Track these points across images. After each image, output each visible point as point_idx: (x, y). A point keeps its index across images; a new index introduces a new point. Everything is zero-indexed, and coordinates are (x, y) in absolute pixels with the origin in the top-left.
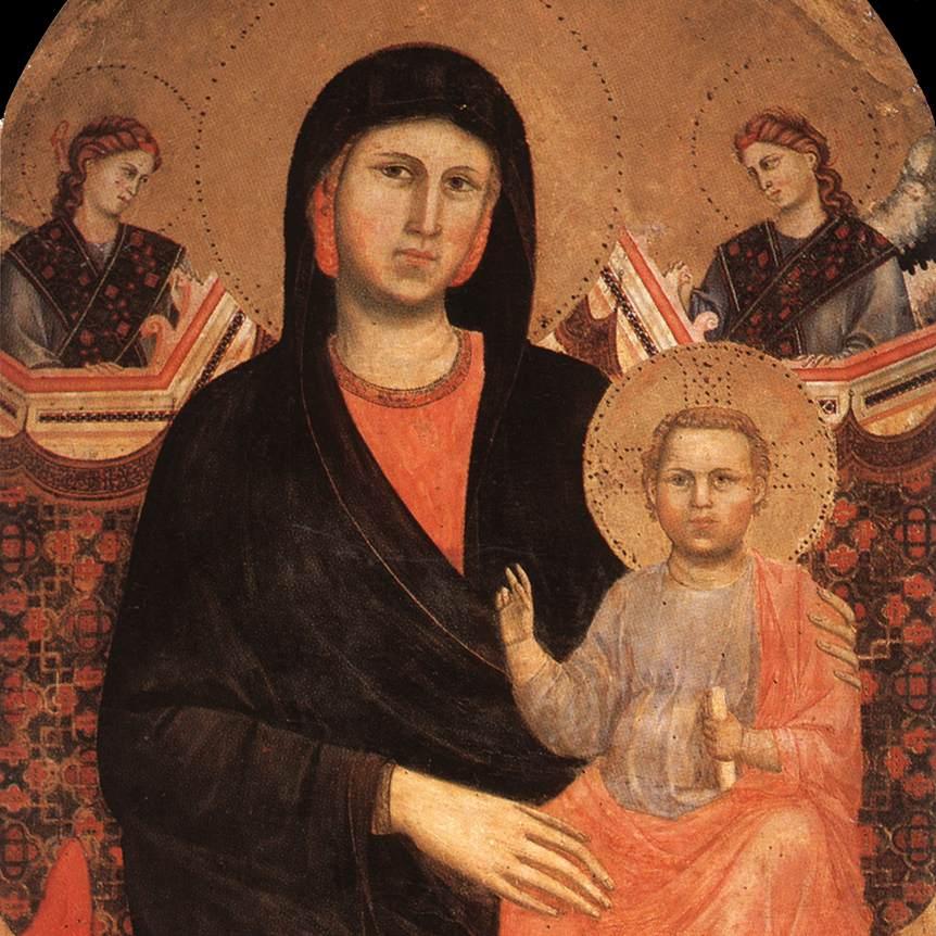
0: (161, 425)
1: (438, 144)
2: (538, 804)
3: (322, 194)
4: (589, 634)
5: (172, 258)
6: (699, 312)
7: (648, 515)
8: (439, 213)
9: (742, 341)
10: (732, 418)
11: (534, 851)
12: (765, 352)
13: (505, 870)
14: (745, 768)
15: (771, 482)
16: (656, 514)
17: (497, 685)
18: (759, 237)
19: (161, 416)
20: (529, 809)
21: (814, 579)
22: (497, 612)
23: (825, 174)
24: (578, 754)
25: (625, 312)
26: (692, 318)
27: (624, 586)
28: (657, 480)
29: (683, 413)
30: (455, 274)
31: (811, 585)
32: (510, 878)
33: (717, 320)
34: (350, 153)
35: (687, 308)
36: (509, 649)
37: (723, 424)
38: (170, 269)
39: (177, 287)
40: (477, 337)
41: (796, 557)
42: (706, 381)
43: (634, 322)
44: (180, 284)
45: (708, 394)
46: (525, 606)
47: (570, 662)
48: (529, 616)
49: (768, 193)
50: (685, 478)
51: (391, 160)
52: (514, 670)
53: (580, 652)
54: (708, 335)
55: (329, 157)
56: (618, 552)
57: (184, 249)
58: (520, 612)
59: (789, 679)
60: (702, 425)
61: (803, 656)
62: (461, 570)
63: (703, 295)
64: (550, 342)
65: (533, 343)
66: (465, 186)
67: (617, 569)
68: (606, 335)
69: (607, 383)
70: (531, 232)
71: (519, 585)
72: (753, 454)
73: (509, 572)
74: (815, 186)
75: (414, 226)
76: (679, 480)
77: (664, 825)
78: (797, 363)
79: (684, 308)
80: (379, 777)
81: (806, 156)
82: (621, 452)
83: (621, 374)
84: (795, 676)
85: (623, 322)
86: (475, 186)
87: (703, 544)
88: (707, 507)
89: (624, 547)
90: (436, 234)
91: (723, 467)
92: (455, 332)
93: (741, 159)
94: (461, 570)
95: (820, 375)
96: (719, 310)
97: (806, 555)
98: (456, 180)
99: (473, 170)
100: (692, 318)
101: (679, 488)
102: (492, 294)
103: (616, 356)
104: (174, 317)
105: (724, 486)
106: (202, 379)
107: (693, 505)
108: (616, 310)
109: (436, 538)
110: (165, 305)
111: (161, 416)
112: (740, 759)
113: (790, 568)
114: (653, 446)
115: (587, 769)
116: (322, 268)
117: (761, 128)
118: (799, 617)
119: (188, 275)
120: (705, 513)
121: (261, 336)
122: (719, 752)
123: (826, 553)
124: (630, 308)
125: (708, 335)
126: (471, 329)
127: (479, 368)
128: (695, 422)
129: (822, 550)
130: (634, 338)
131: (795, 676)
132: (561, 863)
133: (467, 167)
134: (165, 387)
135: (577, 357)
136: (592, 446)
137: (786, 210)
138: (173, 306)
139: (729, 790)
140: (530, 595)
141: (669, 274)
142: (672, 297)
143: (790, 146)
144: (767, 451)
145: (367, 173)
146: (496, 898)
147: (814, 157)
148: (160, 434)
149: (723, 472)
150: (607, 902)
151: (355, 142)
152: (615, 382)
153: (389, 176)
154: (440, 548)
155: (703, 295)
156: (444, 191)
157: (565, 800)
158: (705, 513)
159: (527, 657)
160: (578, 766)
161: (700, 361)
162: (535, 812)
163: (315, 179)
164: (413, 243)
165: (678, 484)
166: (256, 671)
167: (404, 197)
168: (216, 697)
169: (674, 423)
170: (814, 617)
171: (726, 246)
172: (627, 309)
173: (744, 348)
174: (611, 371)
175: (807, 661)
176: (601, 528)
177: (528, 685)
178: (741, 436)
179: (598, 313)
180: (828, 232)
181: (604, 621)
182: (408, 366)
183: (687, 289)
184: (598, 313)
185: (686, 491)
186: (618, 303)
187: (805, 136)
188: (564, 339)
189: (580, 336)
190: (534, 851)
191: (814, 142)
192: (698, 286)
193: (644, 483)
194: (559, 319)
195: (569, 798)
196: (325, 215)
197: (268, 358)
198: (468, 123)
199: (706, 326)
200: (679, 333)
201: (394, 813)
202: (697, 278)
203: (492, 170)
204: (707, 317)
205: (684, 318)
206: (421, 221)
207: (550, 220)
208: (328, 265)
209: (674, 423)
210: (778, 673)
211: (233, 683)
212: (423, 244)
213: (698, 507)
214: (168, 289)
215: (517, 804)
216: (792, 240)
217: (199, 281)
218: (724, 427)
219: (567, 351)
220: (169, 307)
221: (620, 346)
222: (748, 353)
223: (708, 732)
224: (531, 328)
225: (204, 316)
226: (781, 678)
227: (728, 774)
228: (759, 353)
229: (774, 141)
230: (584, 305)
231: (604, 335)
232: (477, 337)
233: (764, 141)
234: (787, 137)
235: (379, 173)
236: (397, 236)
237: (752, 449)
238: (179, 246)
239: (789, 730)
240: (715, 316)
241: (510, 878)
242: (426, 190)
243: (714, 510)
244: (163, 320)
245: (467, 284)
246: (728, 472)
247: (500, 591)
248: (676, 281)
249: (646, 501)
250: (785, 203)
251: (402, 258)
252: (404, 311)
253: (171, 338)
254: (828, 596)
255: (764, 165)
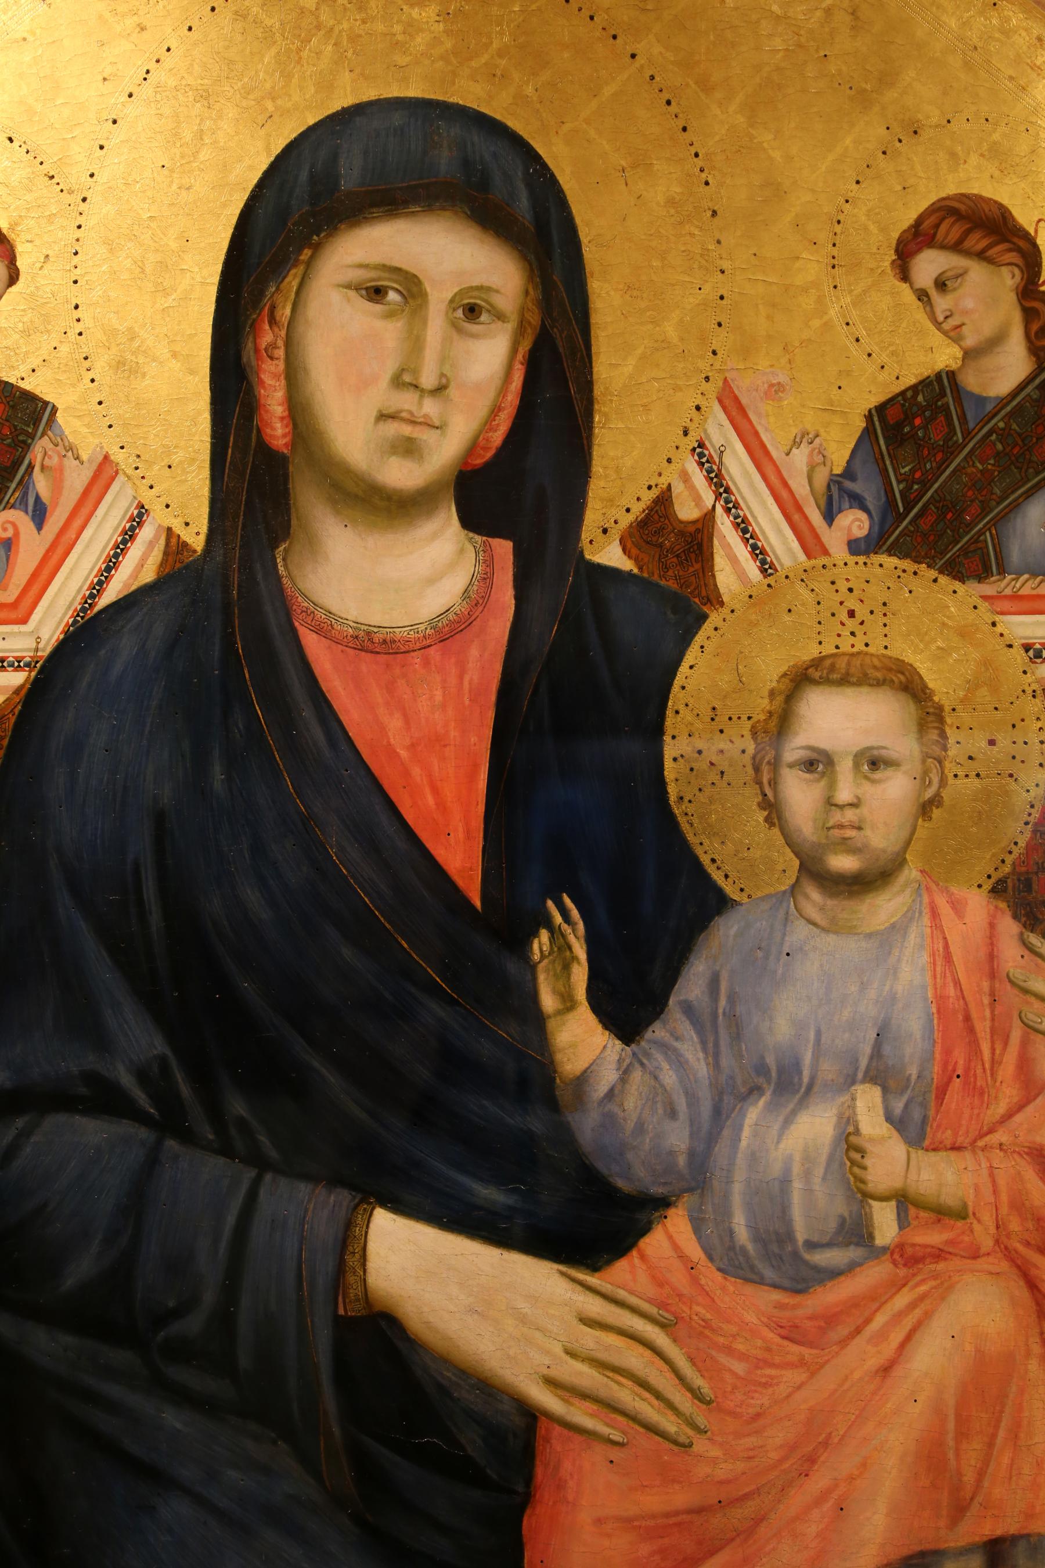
0: (17, 679)
1: (448, 253)
2: (595, 1268)
3: (267, 327)
4: (671, 1002)
5: (36, 422)
6: (840, 511)
7: (761, 819)
8: (443, 359)
9: (904, 555)
10: (890, 670)
11: (590, 1339)
12: (941, 572)
13: (546, 1371)
14: (912, 1211)
15: (950, 768)
16: (774, 815)
17: (535, 1078)
18: (938, 393)
19: (18, 665)
20: (581, 1276)
21: (1015, 917)
22: (533, 968)
23: (1035, 299)
24: (657, 1190)
25: (728, 511)
26: (829, 517)
27: (726, 930)
28: (775, 765)
29: (817, 662)
30: (473, 448)
31: (1009, 927)
32: (551, 1383)
33: (867, 525)
34: (309, 264)
35: (823, 502)
36: (551, 1024)
37: (878, 681)
38: (32, 436)
39: (43, 468)
40: (504, 548)
41: (988, 885)
42: (851, 614)
43: (743, 526)
44: (47, 462)
45: (853, 634)
46: (575, 958)
47: (643, 1043)
48: (580, 975)
49: (946, 326)
50: (817, 763)
51: (373, 274)
52: (559, 1057)
53: (657, 1032)
54: (855, 547)
55: (278, 266)
56: (717, 877)
57: (54, 410)
58: (566, 967)
59: (979, 1071)
60: (844, 681)
61: (1000, 1034)
62: (478, 903)
63: (848, 484)
64: (611, 555)
65: (588, 557)
66: (484, 317)
67: (721, 903)
68: (700, 545)
69: (704, 617)
70: (587, 385)
71: (565, 926)
72: (922, 727)
73: (550, 903)
74: (1017, 317)
75: (407, 378)
76: (810, 765)
77: (787, 1301)
78: (988, 589)
79: (819, 508)
80: (349, 1225)
81: (1005, 270)
82: (722, 720)
83: (722, 604)
84: (987, 1066)
85: (724, 524)
86: (500, 316)
87: (843, 863)
88: (851, 805)
89: (727, 868)
90: (439, 390)
91: (875, 744)
92: (470, 540)
93: (904, 274)
94: (478, 903)
95: (1025, 605)
96: (871, 507)
97: (1002, 881)
98: (472, 309)
99: (497, 291)
100: (829, 517)
101: (807, 776)
102: (522, 482)
103: (714, 576)
104: (39, 515)
105: (878, 775)
106: (84, 610)
107: (830, 803)
108: (714, 507)
109: (440, 853)
110: (25, 494)
111: (18, 665)
112: (905, 1201)
113: (978, 904)
114: (770, 712)
115: (671, 1212)
116: (267, 439)
117: (937, 226)
118: (993, 975)
119: (60, 448)
120: (850, 815)
121: (174, 546)
122: (871, 1187)
123: (1035, 878)
124: (736, 506)
125: (855, 547)
126: (493, 537)
127: (506, 597)
128: (835, 676)
129: (1027, 873)
130: (742, 552)
131: (987, 1066)
132: (635, 1359)
133: (489, 289)
134: (24, 621)
135: (656, 578)
136: (677, 712)
137: (969, 355)
138: (38, 498)
139: (884, 1249)
140: (583, 941)
141: (794, 450)
142: (800, 487)
143: (981, 256)
144: (941, 720)
145: (336, 297)
146: (531, 1415)
147: (1017, 271)
148: (17, 691)
149: (875, 752)
150: (701, 1421)
151: (317, 248)
152: (714, 618)
153: (370, 300)
154: (445, 867)
155: (848, 484)
156: (455, 325)
157: (637, 1261)
158: (850, 815)
159: (580, 1040)
160: (656, 1209)
161: (843, 586)
162: (592, 1280)
163: (256, 301)
164: (406, 401)
165: (809, 771)
166: (163, 1060)
167: (390, 333)
168: (103, 1099)
169: (802, 679)
170: (1017, 974)
171: (881, 408)
172: (731, 507)
173: (906, 564)
174: (708, 601)
175: (1006, 1043)
176: (690, 838)
177: (582, 1080)
178: (902, 696)
179: (686, 511)
180: (1037, 387)
181: (692, 984)
182: (394, 584)
183: (821, 478)
184: (686, 511)
185: (818, 781)
186: (718, 496)
187: (1004, 240)
188: (634, 551)
189: (661, 546)
190: (590, 1339)
191: (1019, 250)
192: (838, 470)
193: (757, 769)
194: (626, 521)
195: (643, 1257)
196: (272, 358)
197: (179, 571)
198: (489, 217)
199: (849, 529)
200: (812, 545)
201: (371, 1280)
202: (839, 458)
203: (527, 293)
204: (851, 518)
205: (816, 517)
206: (416, 372)
207: (613, 367)
208: (277, 432)
209: (802, 679)
210: (961, 1062)
211: (127, 1080)
212: (420, 404)
213: (836, 805)
214: (31, 467)
215: (562, 1268)
216: (981, 400)
217: (77, 458)
218: (879, 684)
219: (640, 568)
220: (31, 501)
221: (720, 561)
222: (915, 573)
223: (857, 1156)
224: (585, 536)
225: (85, 511)
226: (967, 1070)
227: (885, 1224)
228: (933, 573)
229: (956, 247)
230: (664, 501)
231: (697, 542)
232: (504, 548)
233: (943, 247)
234: (977, 241)
235: (352, 294)
236: (380, 395)
237: (921, 719)
238: (46, 403)
239: (980, 1153)
240: (863, 516)
241: (551, 1383)
242: (425, 322)
243: (864, 811)
244: (21, 519)
245: (488, 466)
246: (883, 752)
247: (535, 934)
248: (805, 460)
249: (760, 798)
250: (970, 342)
251: (392, 429)
252: (389, 508)
253: (32, 545)
254: (1039, 945)
255: (941, 285)
